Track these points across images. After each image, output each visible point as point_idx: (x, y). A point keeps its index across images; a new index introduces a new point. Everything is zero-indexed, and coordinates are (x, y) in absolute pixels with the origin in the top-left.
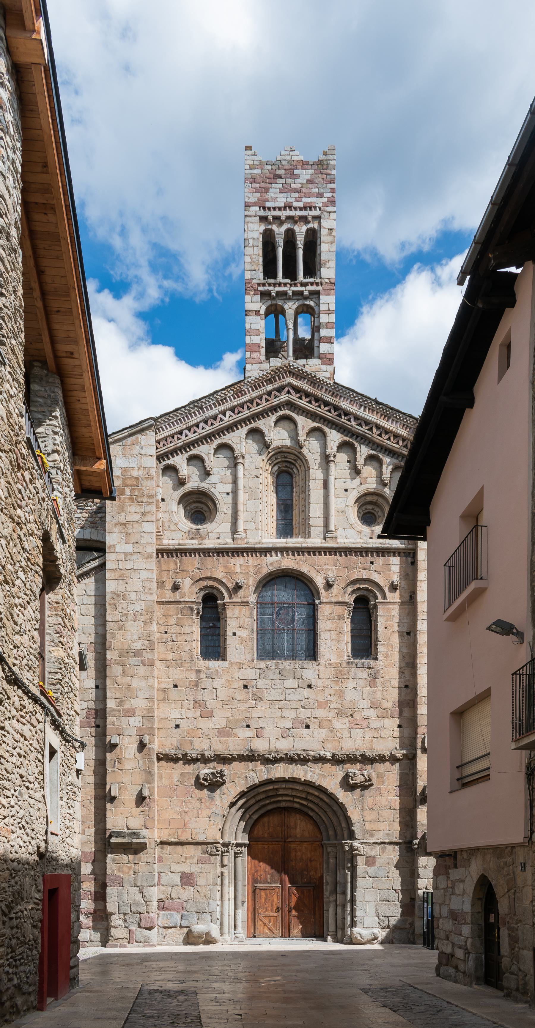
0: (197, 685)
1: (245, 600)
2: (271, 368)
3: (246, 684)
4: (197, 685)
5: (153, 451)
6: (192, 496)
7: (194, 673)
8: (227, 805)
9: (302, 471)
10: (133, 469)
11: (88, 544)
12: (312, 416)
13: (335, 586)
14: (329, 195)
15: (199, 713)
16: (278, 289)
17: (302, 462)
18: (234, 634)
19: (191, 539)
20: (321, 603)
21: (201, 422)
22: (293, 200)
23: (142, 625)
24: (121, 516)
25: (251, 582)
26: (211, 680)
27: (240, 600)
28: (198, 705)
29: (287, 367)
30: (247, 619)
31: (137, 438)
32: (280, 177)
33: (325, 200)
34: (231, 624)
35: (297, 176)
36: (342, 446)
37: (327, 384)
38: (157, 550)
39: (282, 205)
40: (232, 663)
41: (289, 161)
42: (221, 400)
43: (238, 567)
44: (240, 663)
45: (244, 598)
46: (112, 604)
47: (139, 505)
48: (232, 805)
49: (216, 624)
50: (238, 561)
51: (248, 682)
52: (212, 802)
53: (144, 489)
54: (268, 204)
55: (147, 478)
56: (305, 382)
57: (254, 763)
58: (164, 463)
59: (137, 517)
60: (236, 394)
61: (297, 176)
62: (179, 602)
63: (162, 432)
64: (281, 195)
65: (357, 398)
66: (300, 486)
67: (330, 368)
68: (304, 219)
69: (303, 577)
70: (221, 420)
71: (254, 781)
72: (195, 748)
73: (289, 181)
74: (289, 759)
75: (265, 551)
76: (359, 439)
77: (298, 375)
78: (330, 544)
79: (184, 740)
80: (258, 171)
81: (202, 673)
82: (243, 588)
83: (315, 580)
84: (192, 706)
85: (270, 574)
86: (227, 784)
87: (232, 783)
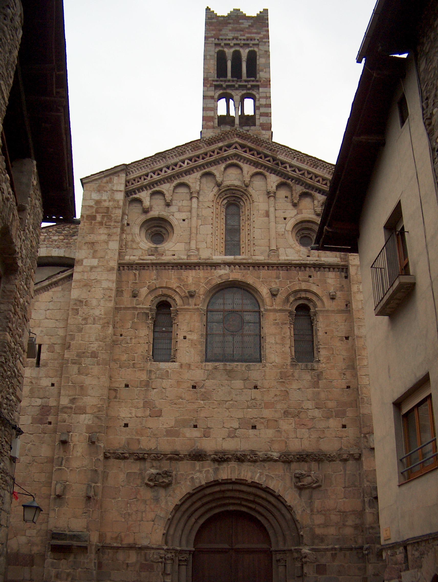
0: (147, 385)
1: (196, 307)
2: (222, 132)
4: (147, 385)
5: (122, 188)
6: (153, 222)
7: (145, 372)
8: (171, 507)
10: (105, 201)
12: (256, 164)
13: (278, 296)
14: (265, 33)
15: (148, 412)
17: (248, 197)
18: (185, 338)
19: (149, 255)
20: (266, 310)
21: (164, 167)
22: (239, 35)
23: (100, 328)
24: (90, 236)
25: (202, 290)
26: (161, 380)
27: (191, 307)
28: (147, 404)
29: (235, 131)
30: (197, 324)
31: (111, 179)
32: (230, 23)
33: (262, 36)
34: (182, 328)
35: (242, 23)
36: (280, 185)
37: (267, 143)
38: (119, 264)
39: (231, 38)
41: (236, 16)
42: (181, 153)
43: (190, 280)
44: (189, 365)
45: (195, 305)
46: (74, 309)
47: (107, 228)
48: (177, 508)
49: (169, 328)
51: (196, 383)
53: (113, 215)
54: (220, 37)
55: (115, 207)
56: (249, 141)
57: (201, 462)
58: (131, 197)
59: (104, 237)
60: (194, 148)
61: (242, 23)
62: (135, 308)
63: (132, 174)
64: (230, 32)
65: (291, 153)
66: (246, 215)
67: (269, 133)
68: (247, 45)
69: (249, 288)
70: (181, 166)
71: (200, 482)
72: (142, 447)
73: (236, 26)
75: (215, 265)
77: (243, 137)
78: (273, 260)
79: (132, 439)
81: (153, 373)
82: (195, 296)
83: (259, 290)
85: (219, 285)
86: (173, 486)
87: (178, 485)
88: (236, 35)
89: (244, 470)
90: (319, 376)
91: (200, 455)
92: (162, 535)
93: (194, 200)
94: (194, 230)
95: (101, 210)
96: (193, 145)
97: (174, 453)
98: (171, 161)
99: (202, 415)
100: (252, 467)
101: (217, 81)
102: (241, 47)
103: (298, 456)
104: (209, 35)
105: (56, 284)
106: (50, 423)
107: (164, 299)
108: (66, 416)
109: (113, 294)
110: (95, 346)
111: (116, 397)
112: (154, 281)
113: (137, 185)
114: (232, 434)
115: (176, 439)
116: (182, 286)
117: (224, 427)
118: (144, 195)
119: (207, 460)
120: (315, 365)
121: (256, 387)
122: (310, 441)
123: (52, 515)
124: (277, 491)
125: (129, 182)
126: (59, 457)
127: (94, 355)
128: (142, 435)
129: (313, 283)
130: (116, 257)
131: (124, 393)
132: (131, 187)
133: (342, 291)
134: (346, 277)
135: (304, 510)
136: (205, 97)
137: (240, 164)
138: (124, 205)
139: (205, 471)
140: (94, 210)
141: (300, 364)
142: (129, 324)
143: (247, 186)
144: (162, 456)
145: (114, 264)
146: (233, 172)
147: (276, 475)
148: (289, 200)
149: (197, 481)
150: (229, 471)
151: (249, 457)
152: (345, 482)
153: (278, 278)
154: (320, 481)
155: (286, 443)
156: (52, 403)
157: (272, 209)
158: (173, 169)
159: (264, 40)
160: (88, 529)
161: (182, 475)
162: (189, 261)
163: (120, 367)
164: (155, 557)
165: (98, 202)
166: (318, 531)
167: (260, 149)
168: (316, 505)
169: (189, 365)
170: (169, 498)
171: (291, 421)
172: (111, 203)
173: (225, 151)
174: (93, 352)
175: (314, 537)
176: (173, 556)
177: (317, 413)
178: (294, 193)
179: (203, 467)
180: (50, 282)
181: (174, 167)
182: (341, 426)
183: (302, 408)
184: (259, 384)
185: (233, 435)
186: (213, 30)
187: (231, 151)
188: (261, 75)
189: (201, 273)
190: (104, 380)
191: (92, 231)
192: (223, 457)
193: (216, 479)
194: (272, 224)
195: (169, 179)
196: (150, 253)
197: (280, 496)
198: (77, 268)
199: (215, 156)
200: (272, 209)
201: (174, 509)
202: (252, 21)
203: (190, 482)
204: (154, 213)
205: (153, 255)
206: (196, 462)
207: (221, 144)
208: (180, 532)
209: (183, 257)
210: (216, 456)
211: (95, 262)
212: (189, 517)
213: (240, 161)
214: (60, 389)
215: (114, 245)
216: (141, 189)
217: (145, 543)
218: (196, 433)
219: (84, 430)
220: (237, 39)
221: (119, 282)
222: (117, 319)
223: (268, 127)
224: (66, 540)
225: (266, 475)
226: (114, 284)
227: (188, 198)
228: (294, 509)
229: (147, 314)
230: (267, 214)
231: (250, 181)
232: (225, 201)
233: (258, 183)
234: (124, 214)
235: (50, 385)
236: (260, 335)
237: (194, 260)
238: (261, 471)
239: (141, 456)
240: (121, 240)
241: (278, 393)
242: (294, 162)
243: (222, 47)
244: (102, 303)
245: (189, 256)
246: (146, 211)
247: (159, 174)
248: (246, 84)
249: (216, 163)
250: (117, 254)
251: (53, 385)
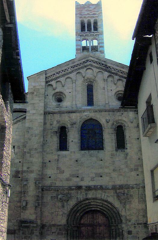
3: (76, 160)
5: (44, 80)
7: (57, 156)
9: (96, 84)
10: (37, 86)
11: (21, 110)
15: (58, 172)
16: (85, 34)
28: (58, 168)
32: (86, 8)
35: (91, 7)
40: (71, 152)
43: (74, 117)
44: (75, 152)
50: (73, 116)
51: (77, 159)
53: (41, 92)
54: (82, 14)
61: (91, 7)
71: (80, 199)
73: (88, 8)
74: (96, 188)
76: (115, 74)
80: (79, 7)
84: (56, 168)
88: (88, 13)
90: (127, 154)
93: (74, 84)
94: (74, 97)
95: (36, 90)
96: (72, 61)
98: (63, 69)
99: (80, 172)
101: (81, 33)
102: (90, 18)
104: (78, 13)
105: (19, 121)
106: (20, 177)
107: (63, 125)
108: (25, 174)
109: (43, 124)
110: (36, 146)
111: (45, 166)
112: (59, 118)
113: (50, 79)
114: (92, 179)
115: (70, 182)
116: (70, 120)
117: (89, 177)
118: (53, 83)
120: (125, 150)
121: (101, 160)
123: (22, 214)
124: (111, 202)
125: (47, 78)
126: (24, 191)
127: (36, 149)
128: (56, 181)
129: (124, 117)
130: (43, 109)
131: (48, 164)
132: (47, 80)
133: (135, 119)
134: (137, 114)
136: (76, 40)
137: (92, 68)
138: (45, 87)
140: (33, 90)
141: (119, 150)
142: (49, 136)
143: (95, 77)
145: (42, 112)
146: (89, 71)
148: (113, 82)
152: (139, 197)
153: (109, 115)
156: (20, 170)
157: (106, 86)
158: (65, 71)
159: (100, 14)
160: (36, 219)
162: (73, 110)
163: (47, 154)
165: (34, 87)
166: (128, 218)
167: (100, 62)
169: (75, 152)
171: (116, 173)
172: (40, 87)
173: (86, 63)
174: (35, 148)
175: (127, 220)
177: (127, 170)
178: (115, 79)
180: (17, 120)
181: (65, 71)
182: (136, 175)
183: (121, 168)
184: (102, 159)
185: (93, 180)
186: (79, 11)
187: (88, 63)
188: (99, 30)
189: (78, 114)
190: (40, 160)
191: (33, 99)
193: (87, 198)
194: (106, 93)
195: (63, 76)
196: (57, 107)
197: (112, 204)
198: (27, 114)
199: (82, 65)
200: (106, 86)
202: (95, 6)
204: (57, 90)
205: (58, 107)
207: (84, 60)
209: (70, 109)
211: (34, 112)
212: (76, 213)
213: (92, 67)
214: (23, 164)
215: (42, 104)
216: (52, 80)
217: (59, 224)
218: (78, 179)
219: (33, 180)
220: (89, 14)
221: (45, 119)
222: (45, 134)
223: (102, 52)
224: (28, 224)
225: (107, 196)
226: (43, 120)
227: (72, 83)
229: (56, 132)
230: (104, 88)
231: (97, 75)
232: (87, 84)
233: (100, 75)
234: (45, 91)
235: (19, 162)
236: (103, 139)
237: (75, 109)
240: (45, 102)
241: (110, 162)
242: (115, 67)
243: (83, 18)
244: (38, 128)
245: (72, 107)
246: (54, 89)
247: (59, 74)
248: (94, 34)
249: (82, 68)
250: (43, 107)
251: (20, 162)
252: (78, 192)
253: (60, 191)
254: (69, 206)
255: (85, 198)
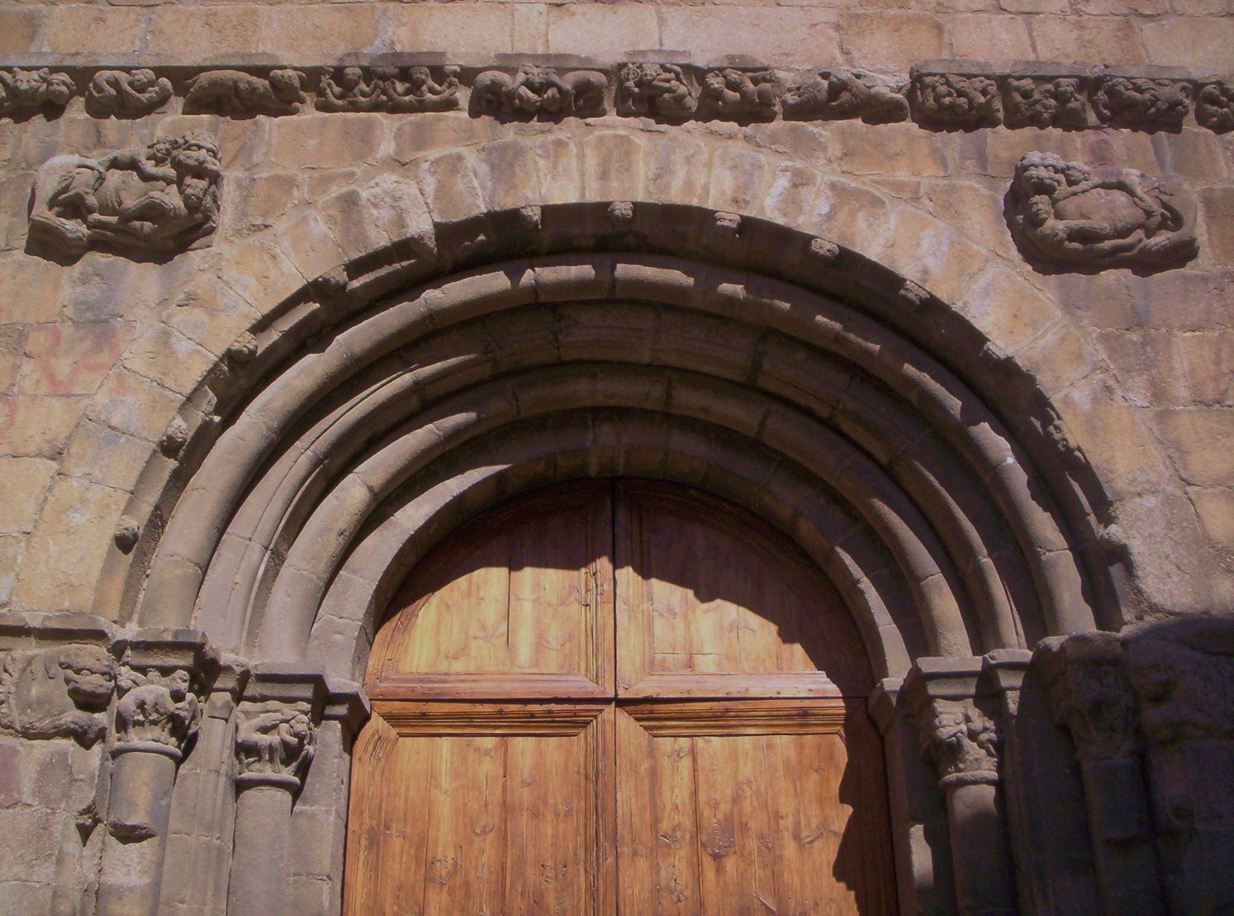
52: (97, 348)
72: (46, 49)
89: (688, 160)
91: (404, 74)
92: (105, 542)
97: (240, 63)
100: (738, 147)
103: (1027, 84)
119: (451, 105)
122: (1080, 27)
124: (907, 270)
135: (1108, 389)
139: (437, 162)
144: (164, 81)
147: (899, 187)
149: (384, 214)
150: (592, 162)
151: (716, 82)
154: (1187, 218)
155: (939, 29)
161: (287, 183)
164: (35, 691)
168: (1181, 364)
170: (181, 317)
176: (178, 696)
179: (421, 139)
192: (555, 78)
193: (507, 203)
197: (932, 306)
201: (211, 378)
203: (330, 219)
206: (378, 116)
208: (256, 558)
210: (505, 77)
225: (833, 186)
228: (1044, 381)
238: (799, 164)
239: (26, 81)
252: (369, 127)
253: (77, 111)
254: (198, 315)
255: (481, 207)
